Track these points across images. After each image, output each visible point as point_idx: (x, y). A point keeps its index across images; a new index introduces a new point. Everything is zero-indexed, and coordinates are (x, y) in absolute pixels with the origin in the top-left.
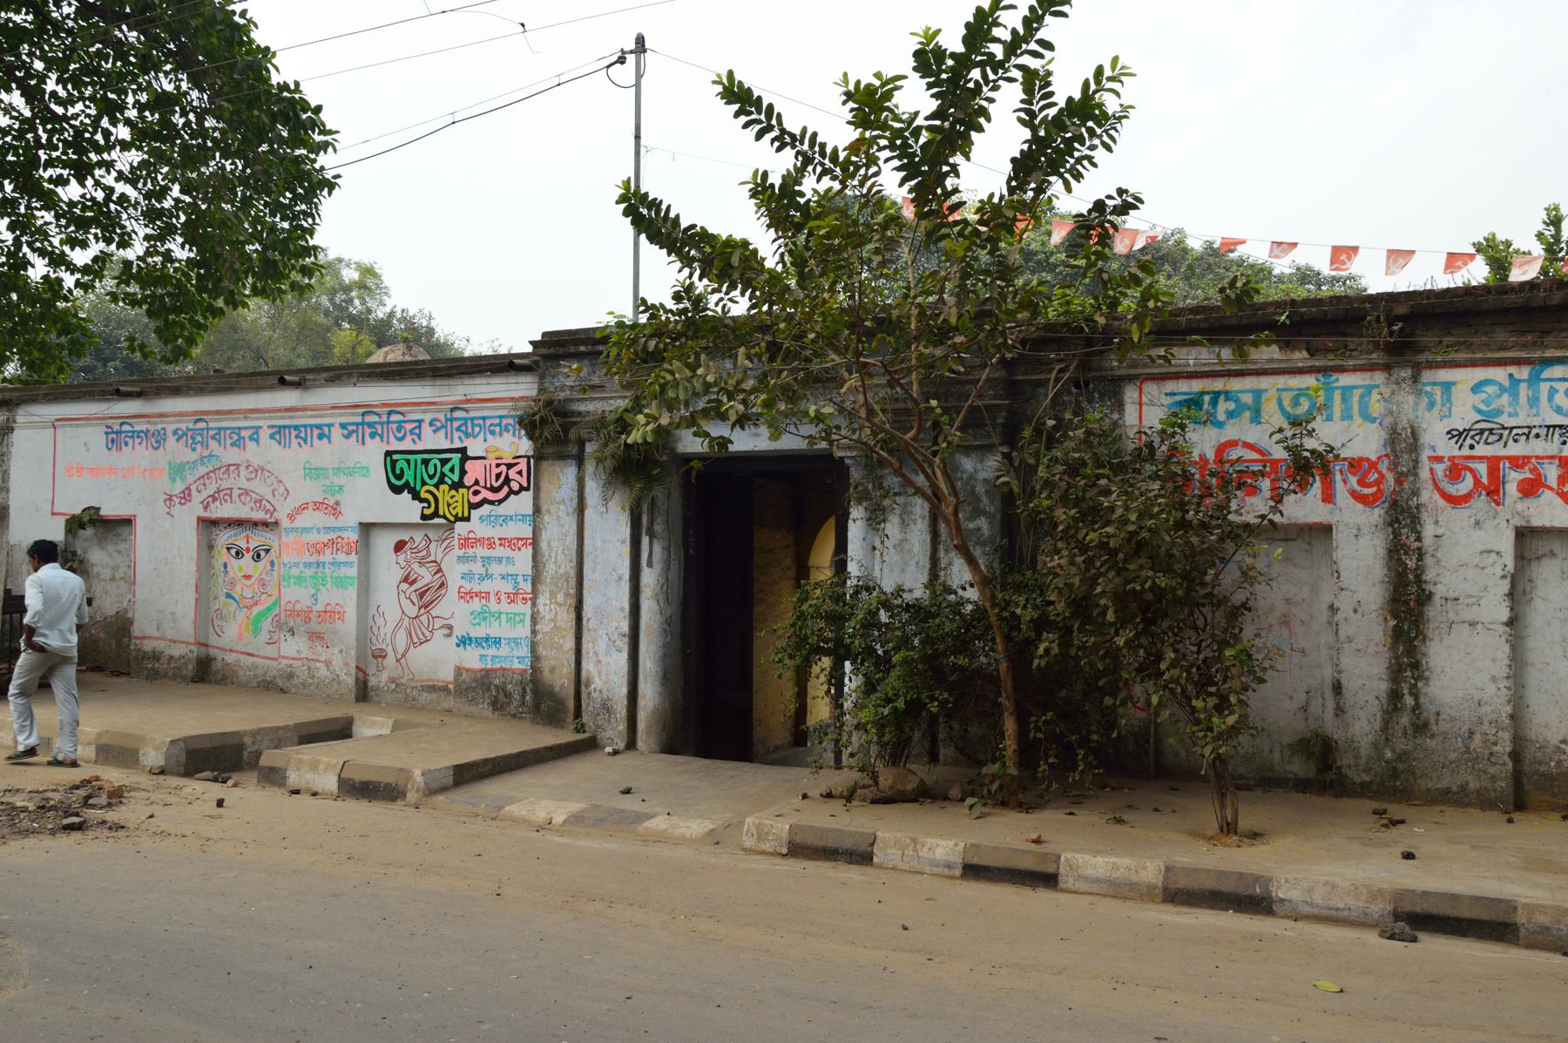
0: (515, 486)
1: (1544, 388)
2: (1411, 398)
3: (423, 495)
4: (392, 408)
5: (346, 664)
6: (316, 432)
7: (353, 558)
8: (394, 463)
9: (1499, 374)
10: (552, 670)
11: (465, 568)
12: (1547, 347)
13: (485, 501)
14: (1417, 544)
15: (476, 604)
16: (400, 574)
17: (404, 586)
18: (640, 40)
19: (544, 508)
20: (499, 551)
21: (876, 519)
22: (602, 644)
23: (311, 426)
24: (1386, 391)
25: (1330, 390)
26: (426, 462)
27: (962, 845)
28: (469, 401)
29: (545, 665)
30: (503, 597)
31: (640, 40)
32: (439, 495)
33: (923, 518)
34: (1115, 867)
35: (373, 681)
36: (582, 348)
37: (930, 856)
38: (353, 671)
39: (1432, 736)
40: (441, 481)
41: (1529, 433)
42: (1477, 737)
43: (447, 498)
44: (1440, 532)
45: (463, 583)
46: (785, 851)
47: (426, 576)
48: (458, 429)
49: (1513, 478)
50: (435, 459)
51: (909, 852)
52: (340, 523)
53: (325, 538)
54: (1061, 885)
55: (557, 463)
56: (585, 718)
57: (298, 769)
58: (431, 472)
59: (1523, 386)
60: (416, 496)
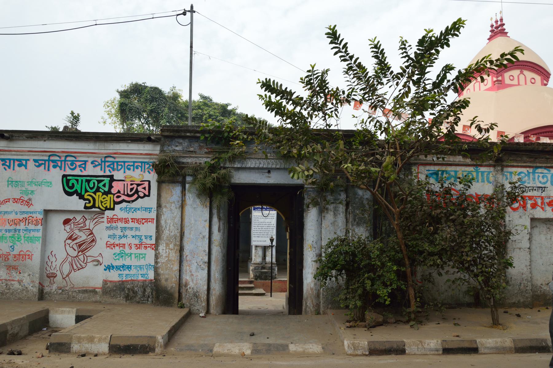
0: (141, 194)
1: (536, 175)
2: (501, 176)
3: (86, 197)
4: (68, 154)
5: (33, 282)
6: (17, 163)
7: (40, 227)
8: (68, 181)
9: (524, 170)
10: (166, 280)
11: (111, 232)
12: (536, 163)
13: (123, 201)
14: (504, 223)
15: (117, 250)
16: (66, 235)
17: (69, 241)
18: (192, 7)
19: (163, 205)
20: (131, 225)
21: (322, 211)
22: (194, 267)
23: (14, 160)
24: (494, 174)
25: (477, 173)
26: (88, 181)
27: (440, 341)
28: (115, 153)
29: (163, 278)
30: (133, 246)
31: (192, 7)
32: (96, 197)
33: (343, 212)
34: (497, 343)
35: (47, 289)
36: (188, 134)
37: (428, 347)
38: (37, 285)
39: (510, 286)
40: (98, 190)
41: (533, 189)
42: (522, 285)
43: (101, 199)
44: (510, 219)
45: (109, 239)
46: (367, 353)
47: (83, 236)
48: (108, 166)
49: (529, 202)
50: (94, 180)
51: (420, 346)
52: (31, 209)
53: (21, 217)
54: (480, 352)
55: (170, 185)
56: (184, 301)
57: (79, 342)
58: (91, 185)
59: (531, 174)
60: (81, 197)
